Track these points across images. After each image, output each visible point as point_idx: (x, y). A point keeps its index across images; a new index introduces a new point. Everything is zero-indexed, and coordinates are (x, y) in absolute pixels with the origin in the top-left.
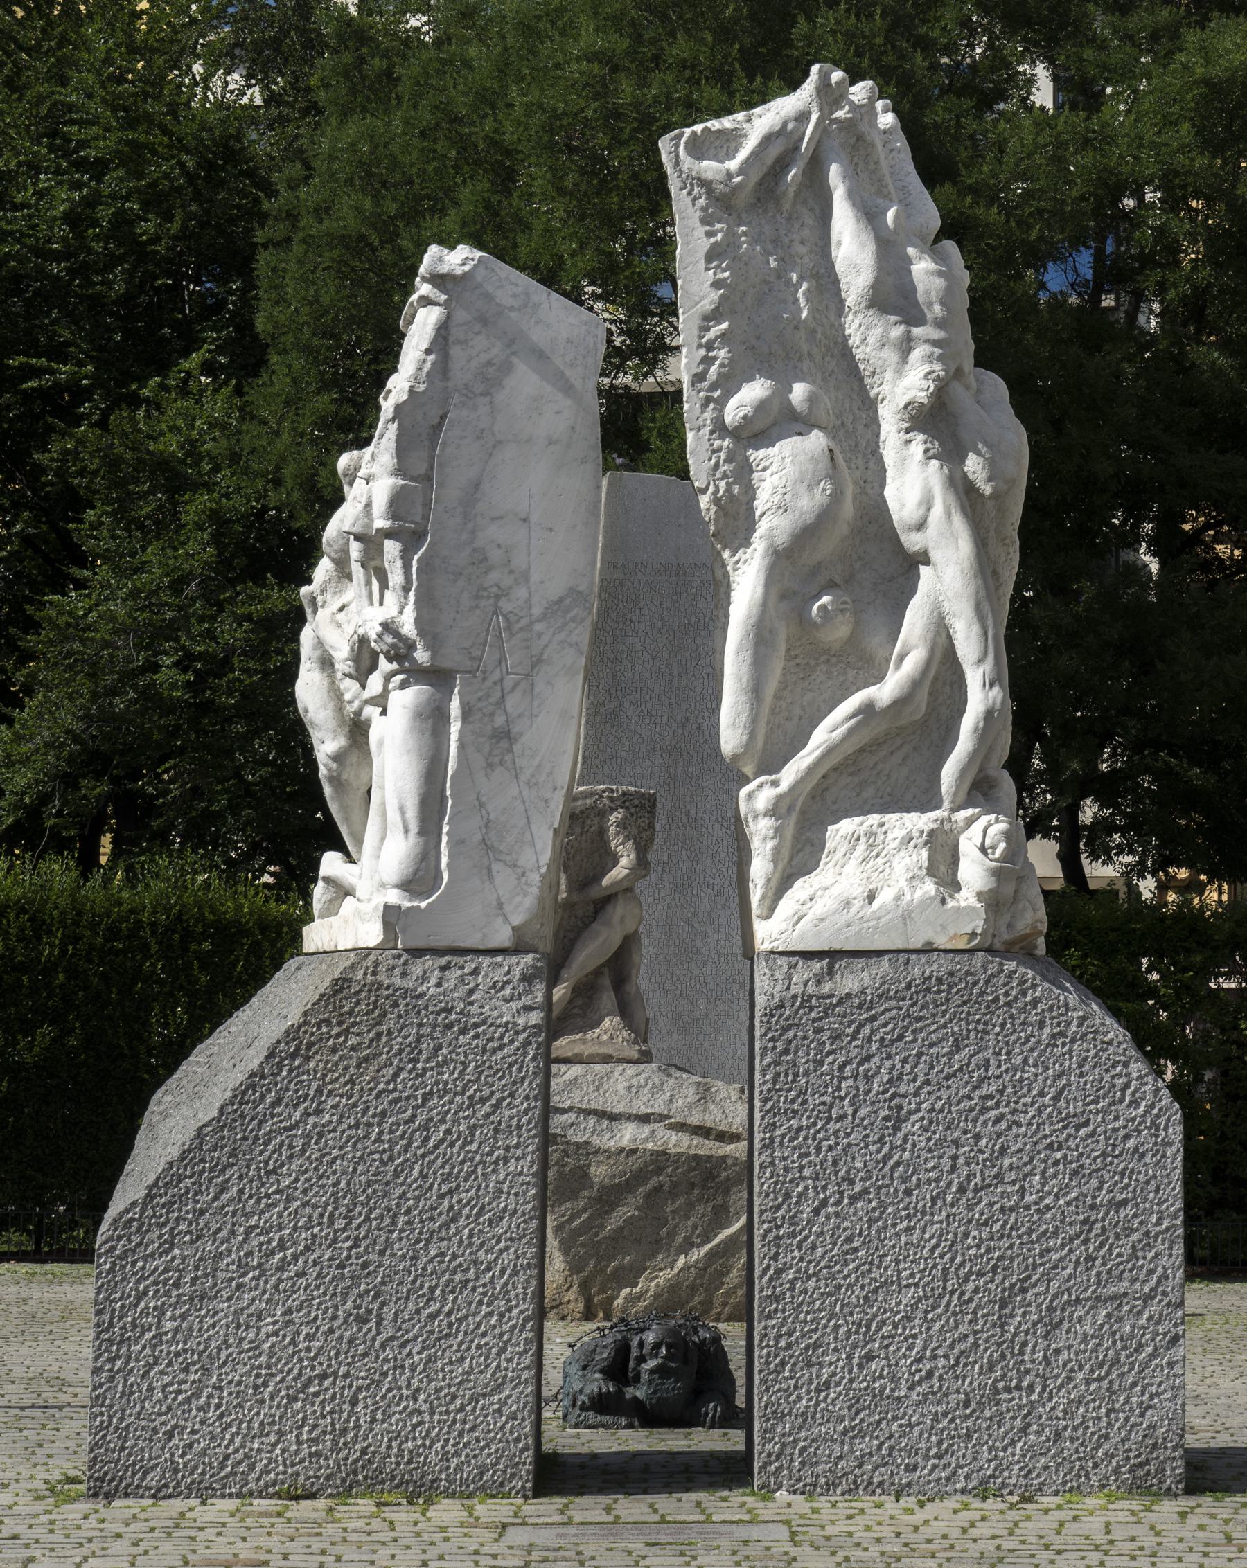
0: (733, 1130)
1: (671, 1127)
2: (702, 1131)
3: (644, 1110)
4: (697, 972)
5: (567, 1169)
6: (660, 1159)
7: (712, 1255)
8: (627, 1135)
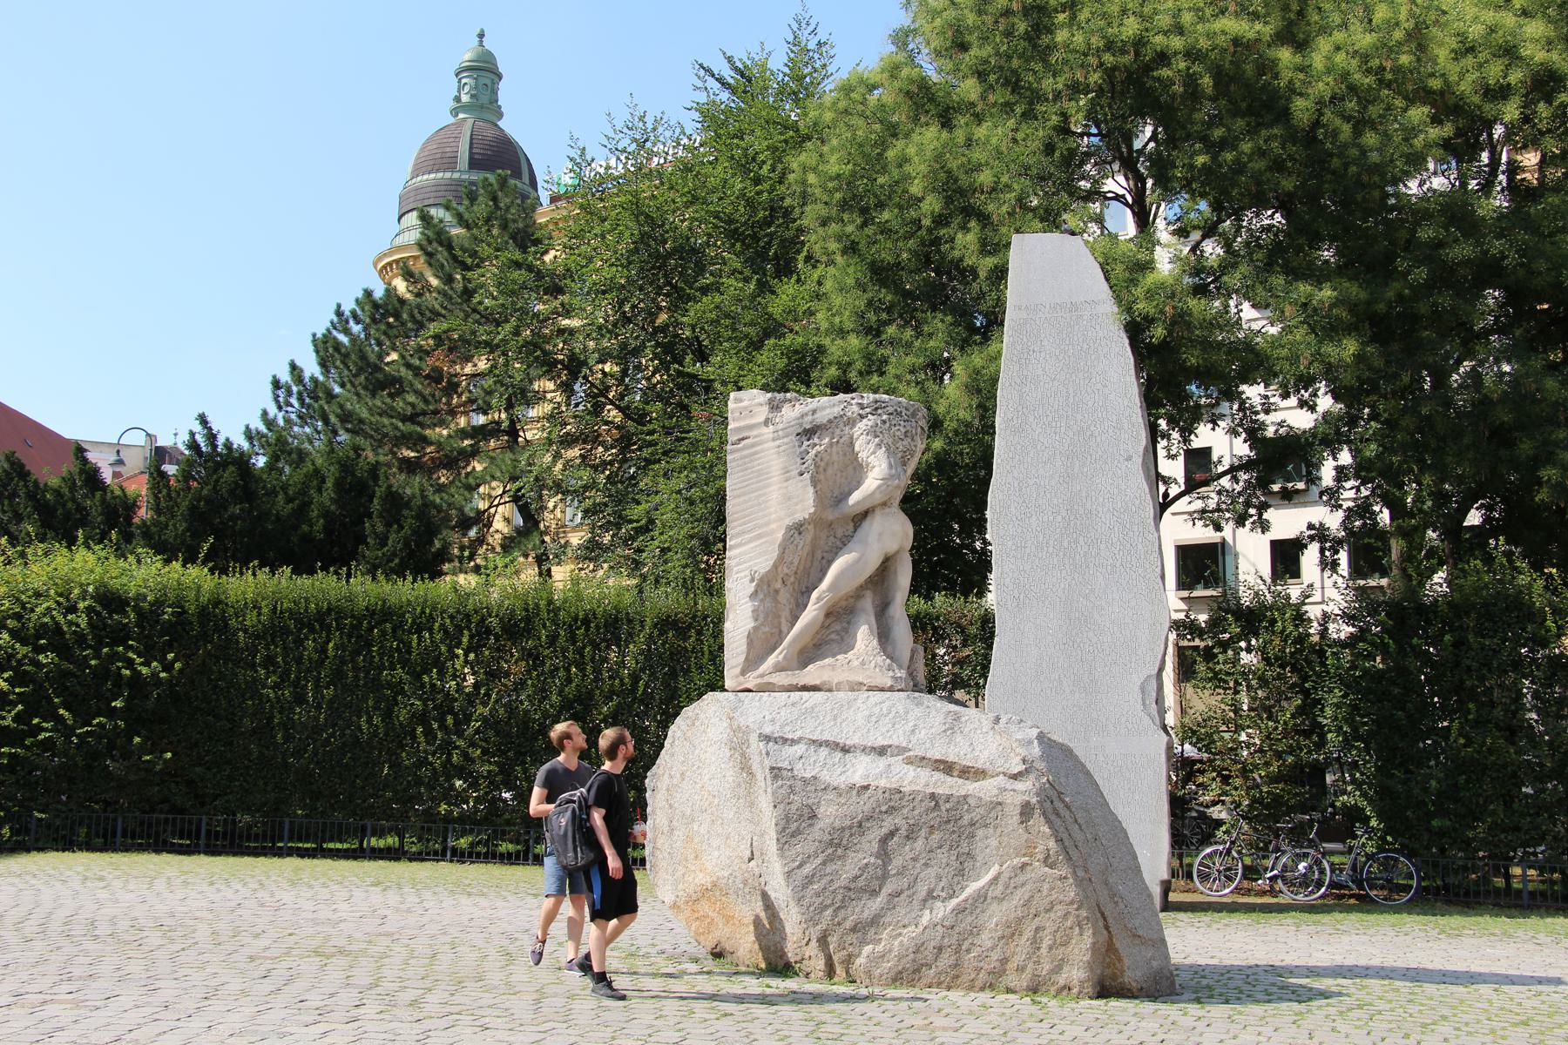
0: (979, 765)
1: (909, 761)
2: (946, 767)
3: (881, 742)
4: (1094, 640)
5: (794, 807)
6: (895, 799)
7: (960, 911)
8: (861, 769)
